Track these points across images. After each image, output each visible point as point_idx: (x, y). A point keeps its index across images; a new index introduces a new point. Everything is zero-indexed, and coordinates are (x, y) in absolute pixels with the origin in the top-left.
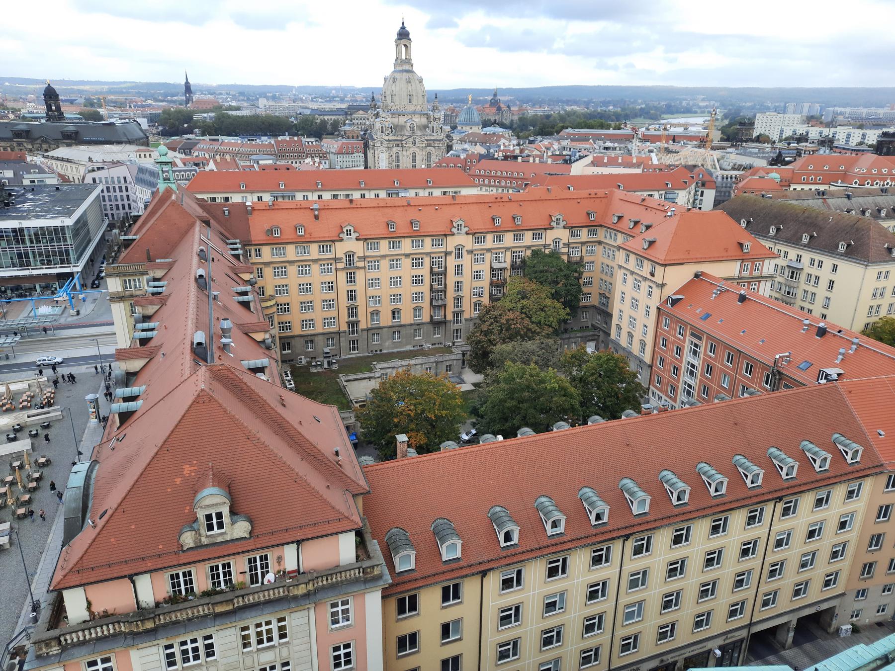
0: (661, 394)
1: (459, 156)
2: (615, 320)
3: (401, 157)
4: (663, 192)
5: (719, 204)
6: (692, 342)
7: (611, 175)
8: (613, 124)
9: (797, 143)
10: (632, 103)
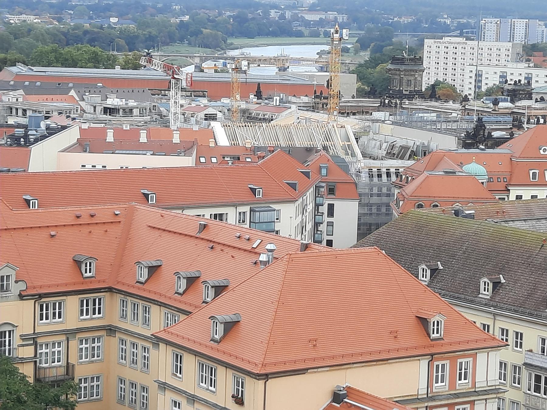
4: (247, 209)
5: (369, 231)
7: (124, 172)
8: (121, 57)
9: (512, 101)
10: (161, 11)
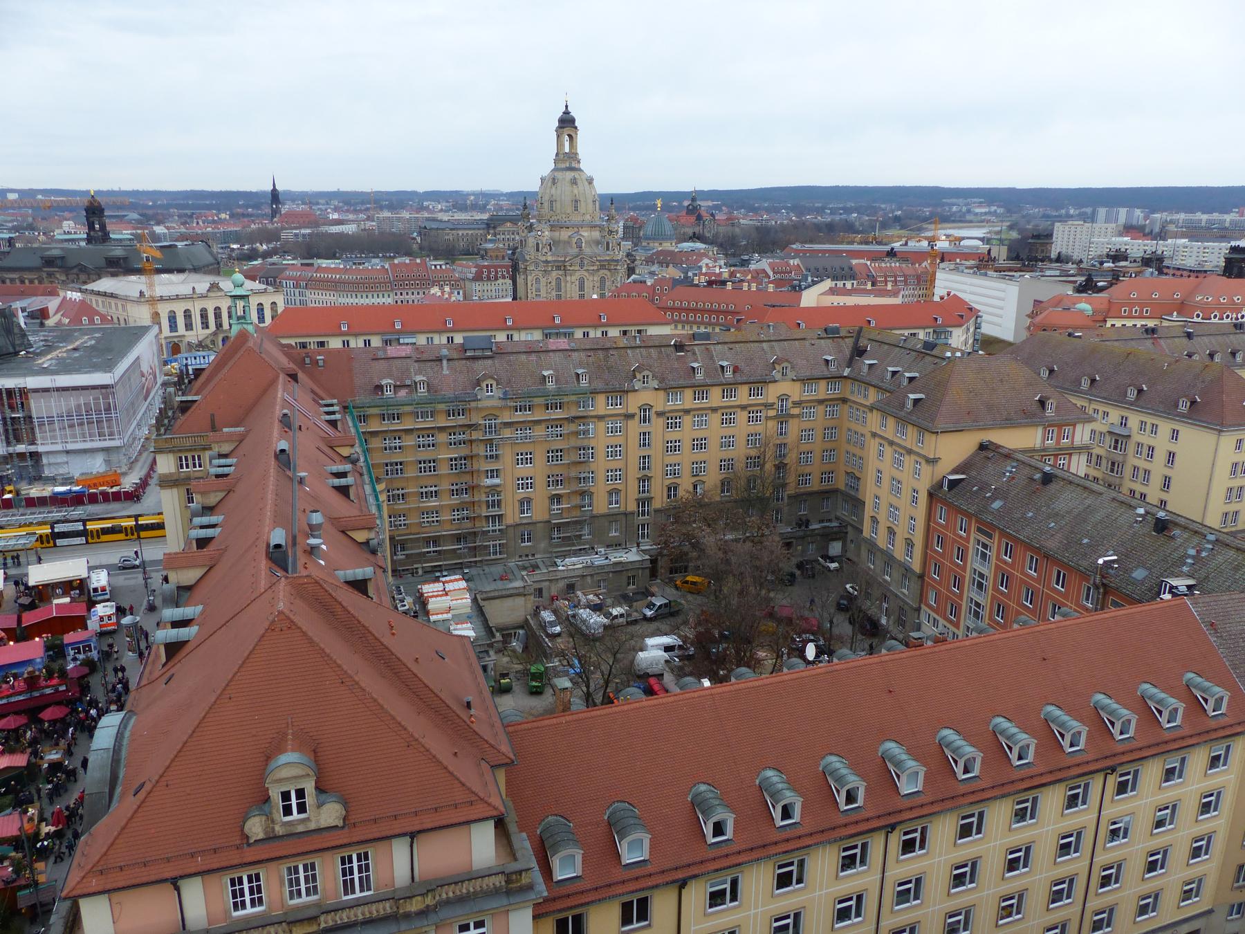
0: (937, 617)
1: (645, 282)
2: (868, 512)
3: (563, 284)
6: (979, 541)
7: (856, 307)
9: (1113, 263)
